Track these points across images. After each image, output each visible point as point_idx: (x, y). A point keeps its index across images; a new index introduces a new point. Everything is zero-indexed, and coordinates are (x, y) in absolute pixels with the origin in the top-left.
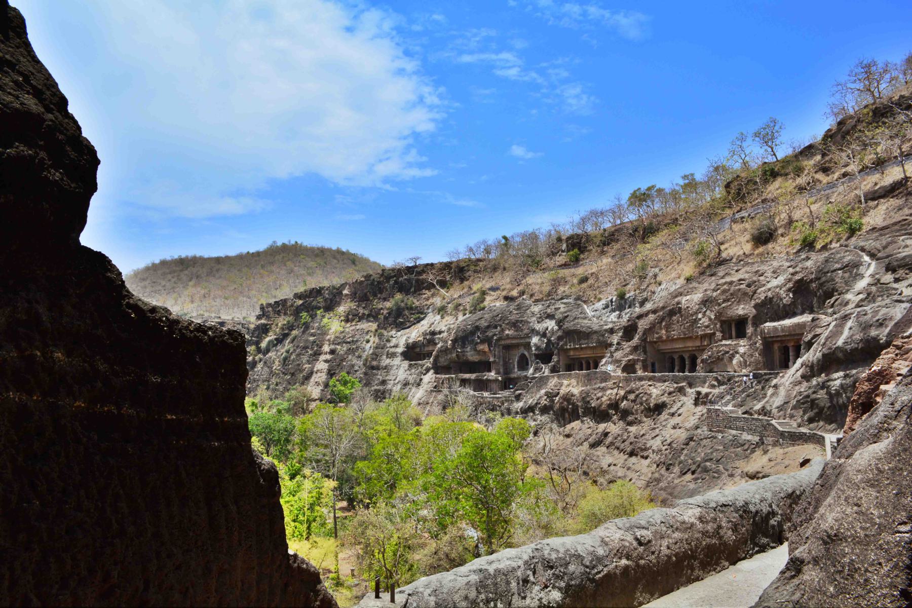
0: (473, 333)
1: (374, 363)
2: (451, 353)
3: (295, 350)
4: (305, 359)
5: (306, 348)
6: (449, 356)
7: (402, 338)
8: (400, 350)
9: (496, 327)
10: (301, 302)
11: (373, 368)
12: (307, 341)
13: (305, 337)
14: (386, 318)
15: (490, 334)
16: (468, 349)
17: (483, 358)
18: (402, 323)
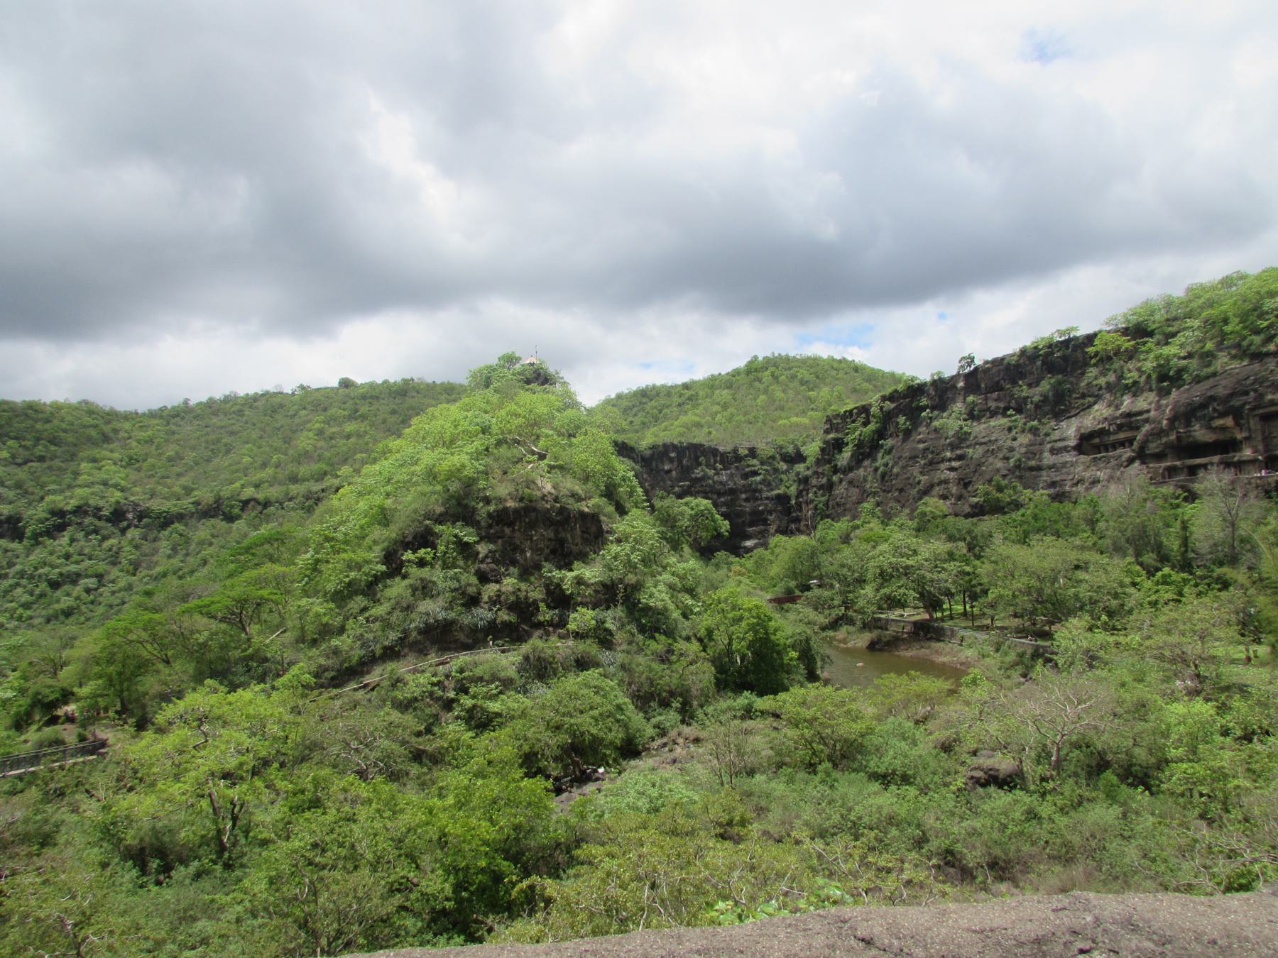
0: (1203, 406)
1: (1033, 463)
2: (1168, 435)
3: (896, 463)
4: (915, 471)
5: (913, 458)
6: (1164, 440)
7: (1070, 430)
8: (1072, 443)
9: (1246, 393)
10: (893, 406)
11: (1031, 469)
12: (914, 449)
13: (909, 445)
14: (1037, 406)
15: (1236, 402)
16: (1197, 427)
17: (1221, 437)
18: (1064, 411)
